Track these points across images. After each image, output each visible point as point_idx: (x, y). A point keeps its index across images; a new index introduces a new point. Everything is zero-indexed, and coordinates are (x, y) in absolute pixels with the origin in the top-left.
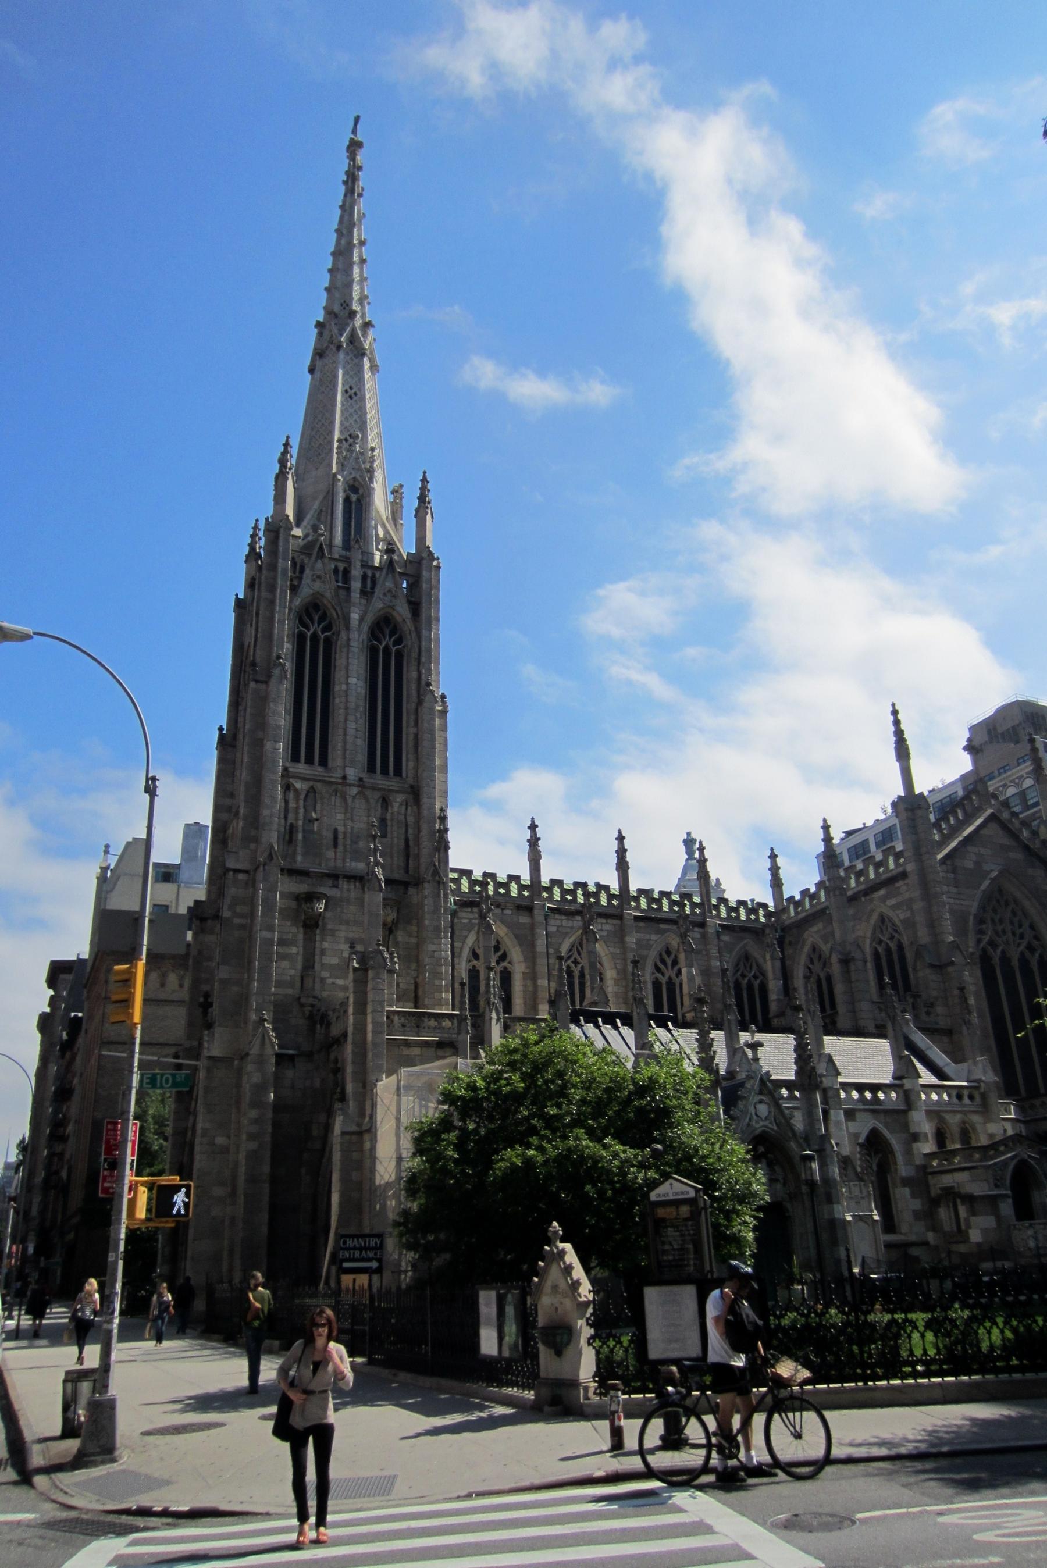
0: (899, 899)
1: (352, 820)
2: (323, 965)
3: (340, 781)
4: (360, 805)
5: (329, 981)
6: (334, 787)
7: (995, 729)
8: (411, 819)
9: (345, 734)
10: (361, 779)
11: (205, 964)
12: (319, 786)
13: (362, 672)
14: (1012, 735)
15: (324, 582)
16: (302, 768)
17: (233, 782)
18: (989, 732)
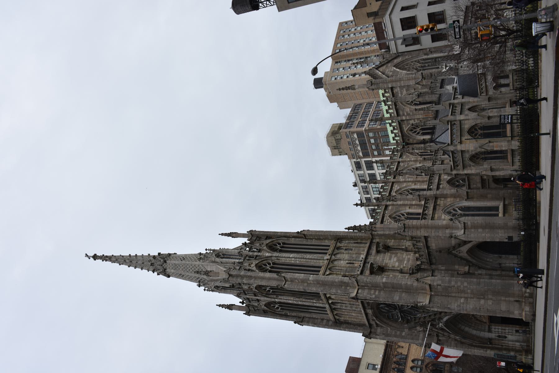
0: (399, 92)
2: (398, 267)
4: (338, 256)
5: (404, 265)
6: (330, 263)
7: (334, 147)
8: (347, 242)
9: (311, 259)
10: (329, 255)
11: (389, 333)
12: (329, 267)
13: (288, 254)
14: (338, 141)
15: (252, 263)
16: (321, 272)
17: (317, 319)
18: (335, 149)
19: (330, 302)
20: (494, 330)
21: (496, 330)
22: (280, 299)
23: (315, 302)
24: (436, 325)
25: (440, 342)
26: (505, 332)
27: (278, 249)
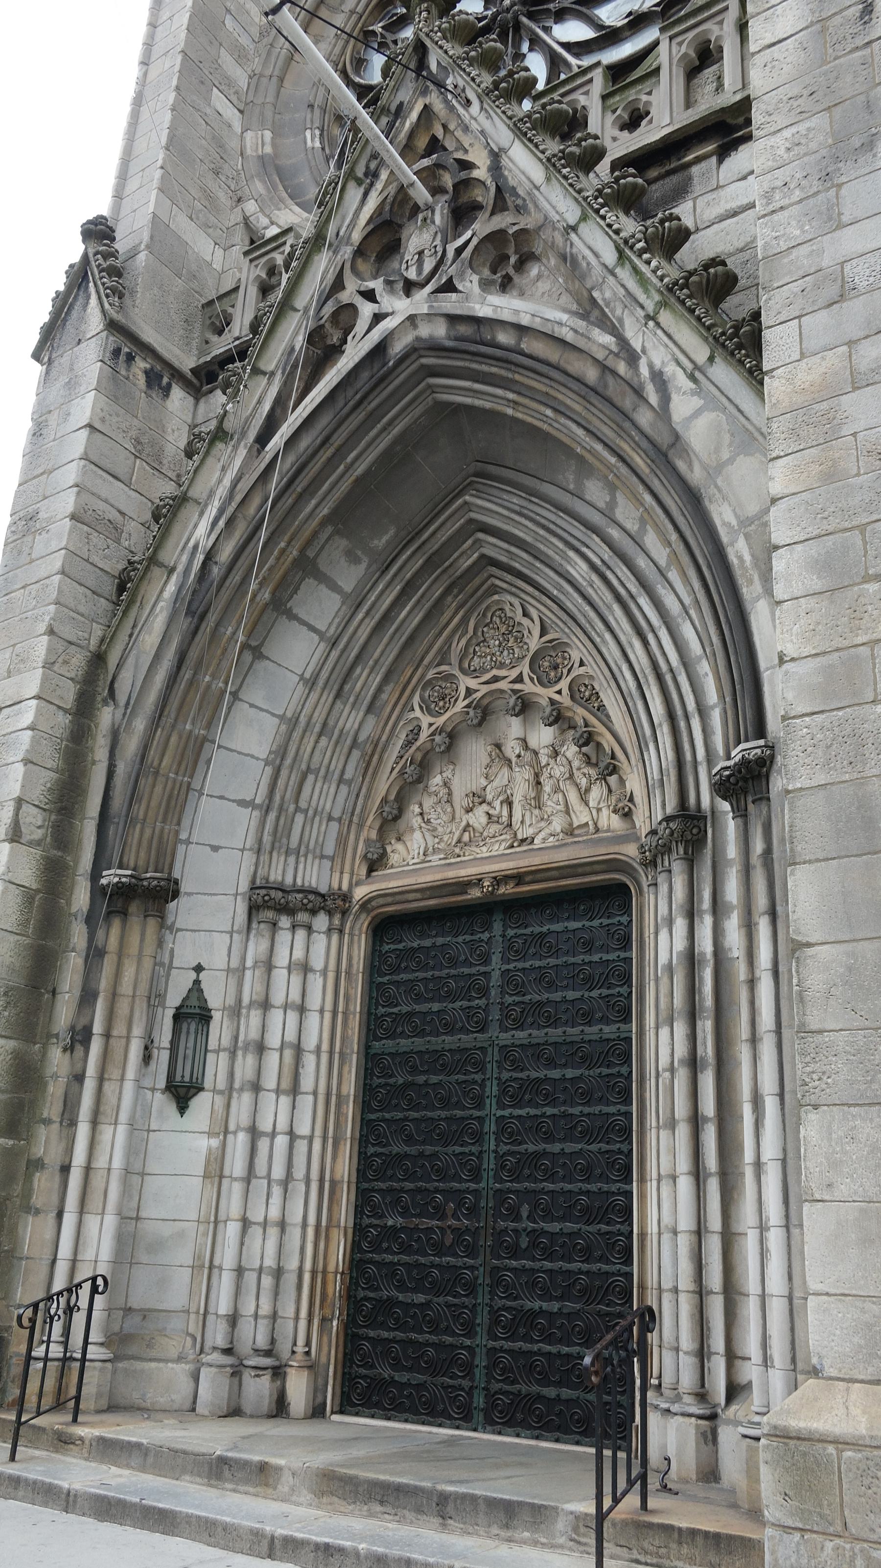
20: (282, 958)
21: (280, 975)
26: (256, 1087)
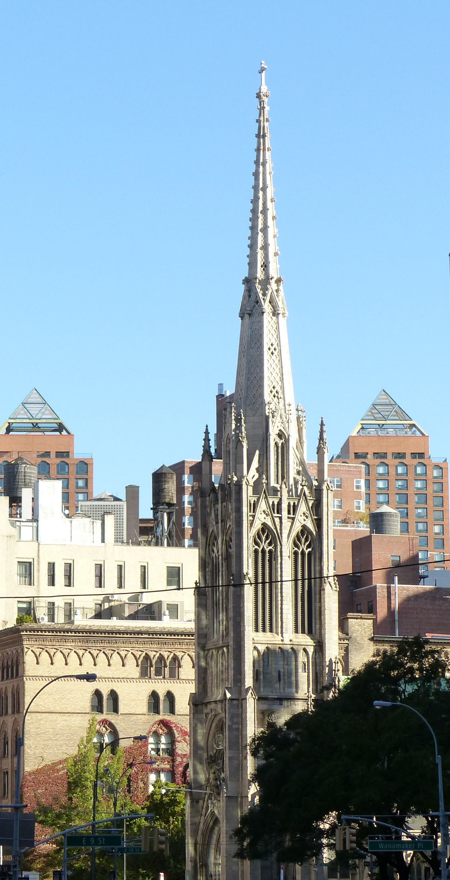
1: (288, 664)
3: (281, 642)
19: (225, 649)
22: (222, 564)
23: (224, 624)
24: (211, 799)
25: (195, 802)
27: (299, 548)
